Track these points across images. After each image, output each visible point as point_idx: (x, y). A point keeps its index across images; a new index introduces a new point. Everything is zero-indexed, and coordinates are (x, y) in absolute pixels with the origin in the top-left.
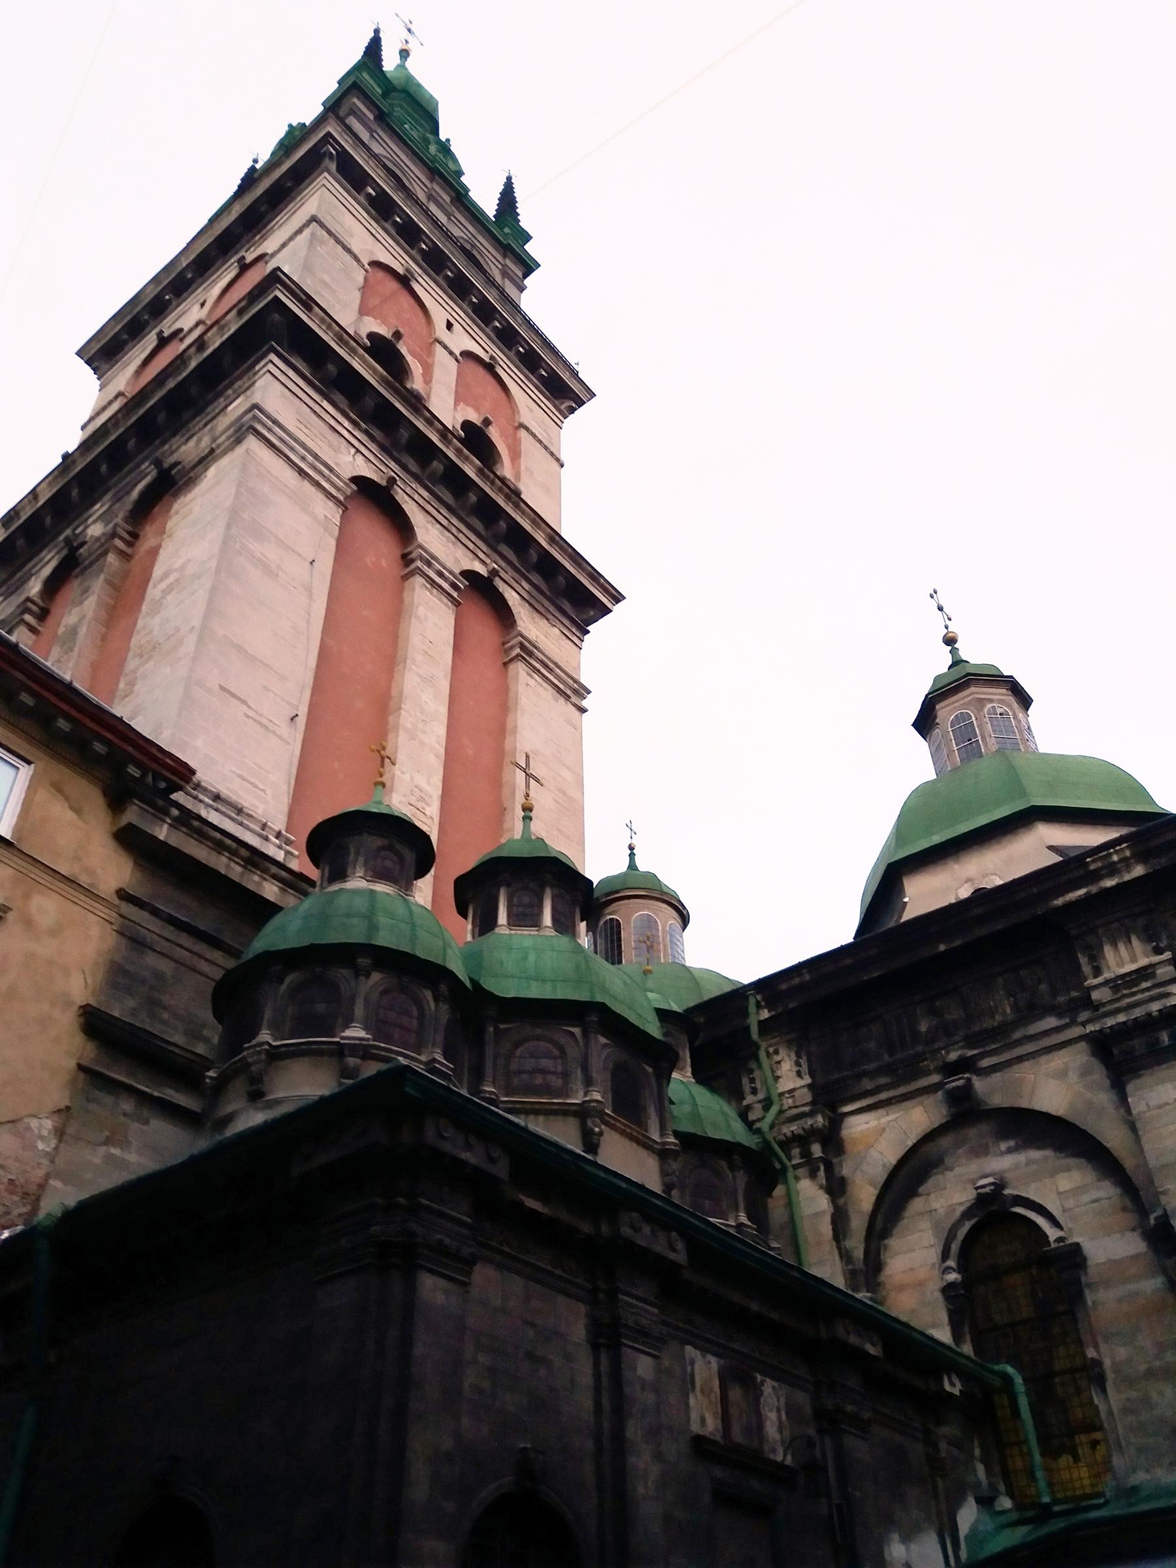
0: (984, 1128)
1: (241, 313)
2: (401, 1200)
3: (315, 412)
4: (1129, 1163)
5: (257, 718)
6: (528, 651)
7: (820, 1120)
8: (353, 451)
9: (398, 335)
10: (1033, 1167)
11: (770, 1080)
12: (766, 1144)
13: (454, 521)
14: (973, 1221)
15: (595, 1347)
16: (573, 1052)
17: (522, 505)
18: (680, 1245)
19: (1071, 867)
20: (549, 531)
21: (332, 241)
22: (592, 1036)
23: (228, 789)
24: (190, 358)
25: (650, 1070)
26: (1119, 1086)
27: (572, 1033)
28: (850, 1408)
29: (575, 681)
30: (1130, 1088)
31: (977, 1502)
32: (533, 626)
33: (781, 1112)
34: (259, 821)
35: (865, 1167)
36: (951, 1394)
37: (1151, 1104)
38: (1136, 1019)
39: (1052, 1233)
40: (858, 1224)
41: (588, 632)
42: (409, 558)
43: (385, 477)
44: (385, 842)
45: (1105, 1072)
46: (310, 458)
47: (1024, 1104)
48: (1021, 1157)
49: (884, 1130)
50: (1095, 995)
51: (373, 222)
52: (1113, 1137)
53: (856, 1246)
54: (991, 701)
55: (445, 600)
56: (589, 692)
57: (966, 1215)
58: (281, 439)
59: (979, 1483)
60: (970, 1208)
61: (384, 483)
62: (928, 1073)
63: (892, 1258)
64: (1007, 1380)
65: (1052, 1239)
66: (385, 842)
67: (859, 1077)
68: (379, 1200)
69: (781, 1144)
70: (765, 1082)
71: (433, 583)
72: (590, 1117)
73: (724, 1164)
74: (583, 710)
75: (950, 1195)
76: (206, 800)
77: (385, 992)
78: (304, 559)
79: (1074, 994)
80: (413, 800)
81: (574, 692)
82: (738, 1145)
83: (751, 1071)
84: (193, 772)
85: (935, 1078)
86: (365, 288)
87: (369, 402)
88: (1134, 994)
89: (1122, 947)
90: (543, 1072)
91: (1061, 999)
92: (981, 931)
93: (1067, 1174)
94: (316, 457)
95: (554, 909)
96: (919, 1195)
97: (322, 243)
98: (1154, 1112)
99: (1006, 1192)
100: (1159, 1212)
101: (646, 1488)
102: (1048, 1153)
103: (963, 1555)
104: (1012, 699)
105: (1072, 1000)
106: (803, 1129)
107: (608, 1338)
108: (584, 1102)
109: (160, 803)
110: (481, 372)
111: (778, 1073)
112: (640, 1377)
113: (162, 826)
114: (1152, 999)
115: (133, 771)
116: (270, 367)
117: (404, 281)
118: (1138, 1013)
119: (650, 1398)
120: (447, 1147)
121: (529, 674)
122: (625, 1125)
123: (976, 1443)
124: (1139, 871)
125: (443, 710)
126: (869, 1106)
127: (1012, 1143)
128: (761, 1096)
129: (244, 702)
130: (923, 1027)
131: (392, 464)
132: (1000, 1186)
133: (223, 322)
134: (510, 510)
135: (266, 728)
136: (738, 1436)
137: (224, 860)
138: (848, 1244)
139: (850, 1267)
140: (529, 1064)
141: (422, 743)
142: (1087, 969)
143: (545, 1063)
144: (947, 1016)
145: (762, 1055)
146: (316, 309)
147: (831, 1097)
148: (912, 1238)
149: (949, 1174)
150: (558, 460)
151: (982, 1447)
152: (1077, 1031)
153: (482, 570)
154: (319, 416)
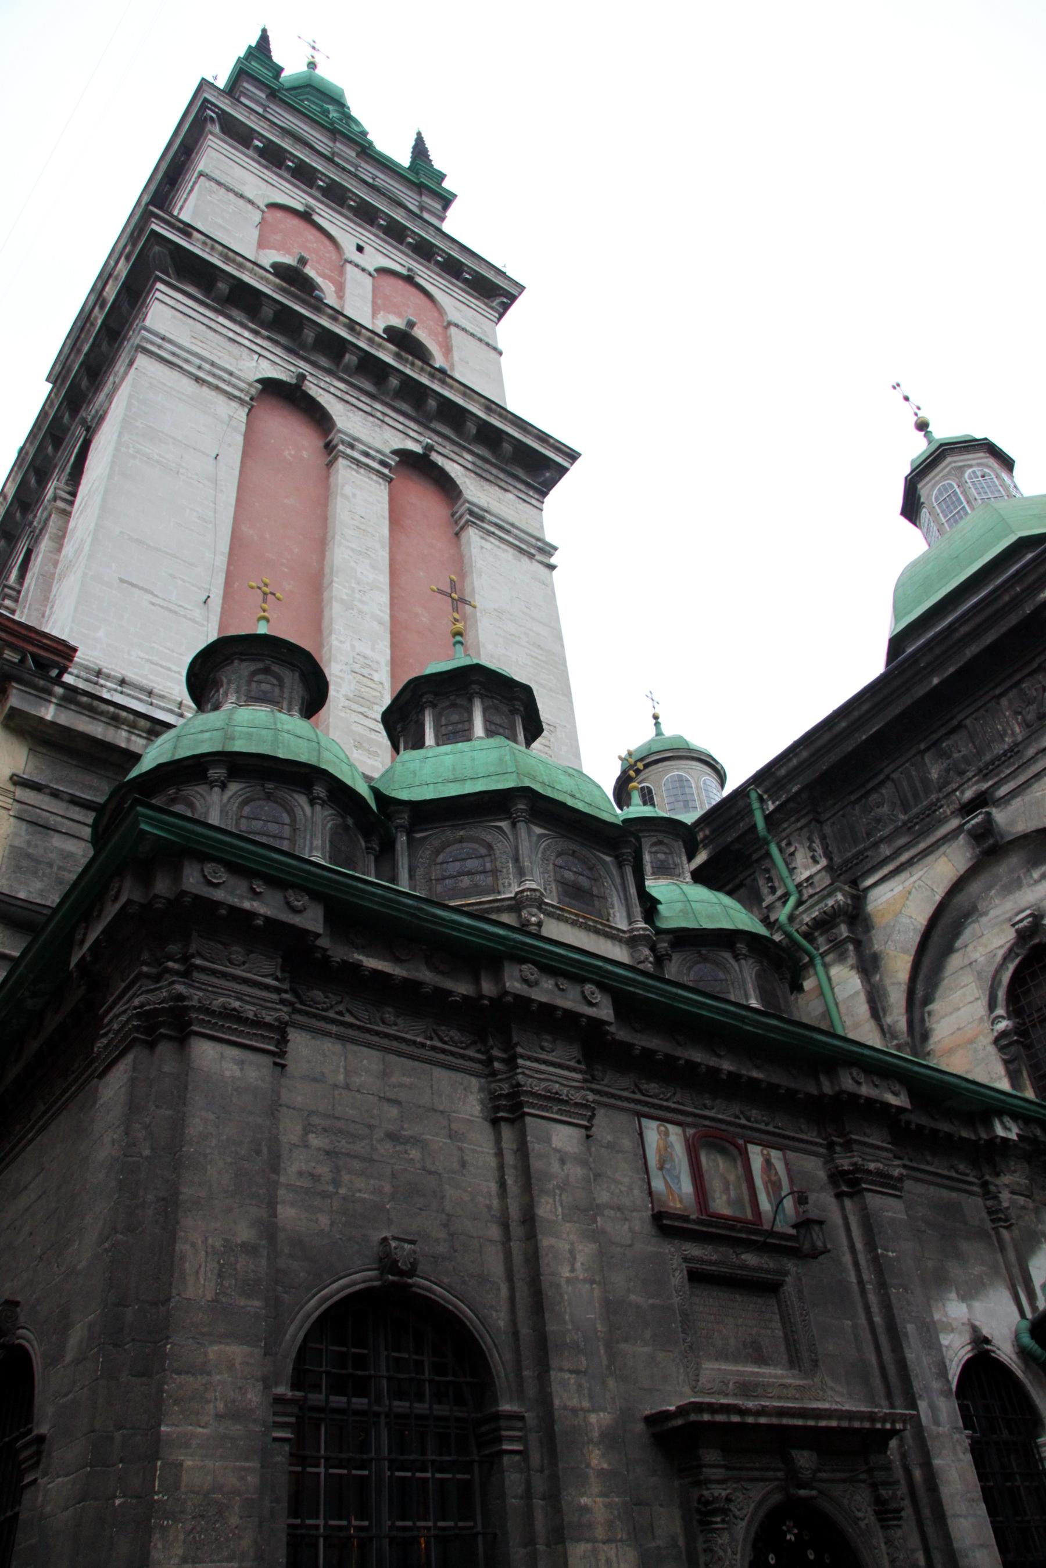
0: (1014, 860)
1: (128, 258)
2: (170, 964)
3: (210, 328)
5: (166, 604)
6: (478, 516)
8: (256, 357)
9: (303, 261)
13: (379, 406)
14: (1017, 961)
15: (495, 1122)
16: (501, 847)
17: (448, 380)
18: (598, 997)
20: (483, 400)
21: (223, 190)
22: (521, 825)
23: (136, 674)
24: (96, 318)
25: (608, 859)
27: (500, 828)
28: (872, 1166)
29: (538, 539)
32: (476, 491)
33: (800, 903)
34: (174, 701)
35: (896, 936)
36: (1005, 1140)
40: (897, 997)
42: (330, 445)
43: (294, 375)
44: (261, 666)
46: (207, 366)
49: (910, 893)
51: (265, 171)
53: (897, 1017)
55: (375, 477)
56: (556, 549)
58: (174, 354)
60: (1011, 950)
61: (294, 381)
62: (942, 821)
63: (938, 1022)
66: (261, 666)
67: (876, 845)
68: (145, 969)
69: (808, 936)
70: (782, 879)
71: (358, 463)
72: (525, 907)
73: (728, 955)
74: (552, 567)
76: (109, 684)
77: (246, 802)
78: (208, 456)
80: (356, 667)
81: (539, 551)
83: (767, 871)
84: (74, 650)
85: (955, 823)
86: (263, 223)
87: (268, 312)
90: (469, 873)
92: (971, 651)
94: (213, 364)
95: (486, 721)
96: (958, 950)
97: (211, 192)
101: (573, 1270)
106: (825, 912)
107: (508, 1110)
108: (517, 893)
109: (41, 683)
110: (400, 284)
112: (556, 1150)
113: (47, 709)
115: (8, 654)
116: (158, 295)
117: (306, 216)
119: (576, 1172)
120: (219, 895)
121: (482, 538)
122: (576, 915)
125: (384, 579)
126: (891, 872)
128: (779, 893)
129: (146, 591)
130: (934, 775)
131: (302, 364)
133: (116, 273)
134: (436, 387)
135: (176, 613)
137: (124, 734)
138: (889, 1020)
139: (895, 1042)
140: (454, 867)
141: (361, 612)
143: (471, 864)
144: (956, 755)
145: (774, 850)
146: (196, 234)
149: (984, 920)
150: (495, 349)
153: (418, 449)
154: (215, 331)
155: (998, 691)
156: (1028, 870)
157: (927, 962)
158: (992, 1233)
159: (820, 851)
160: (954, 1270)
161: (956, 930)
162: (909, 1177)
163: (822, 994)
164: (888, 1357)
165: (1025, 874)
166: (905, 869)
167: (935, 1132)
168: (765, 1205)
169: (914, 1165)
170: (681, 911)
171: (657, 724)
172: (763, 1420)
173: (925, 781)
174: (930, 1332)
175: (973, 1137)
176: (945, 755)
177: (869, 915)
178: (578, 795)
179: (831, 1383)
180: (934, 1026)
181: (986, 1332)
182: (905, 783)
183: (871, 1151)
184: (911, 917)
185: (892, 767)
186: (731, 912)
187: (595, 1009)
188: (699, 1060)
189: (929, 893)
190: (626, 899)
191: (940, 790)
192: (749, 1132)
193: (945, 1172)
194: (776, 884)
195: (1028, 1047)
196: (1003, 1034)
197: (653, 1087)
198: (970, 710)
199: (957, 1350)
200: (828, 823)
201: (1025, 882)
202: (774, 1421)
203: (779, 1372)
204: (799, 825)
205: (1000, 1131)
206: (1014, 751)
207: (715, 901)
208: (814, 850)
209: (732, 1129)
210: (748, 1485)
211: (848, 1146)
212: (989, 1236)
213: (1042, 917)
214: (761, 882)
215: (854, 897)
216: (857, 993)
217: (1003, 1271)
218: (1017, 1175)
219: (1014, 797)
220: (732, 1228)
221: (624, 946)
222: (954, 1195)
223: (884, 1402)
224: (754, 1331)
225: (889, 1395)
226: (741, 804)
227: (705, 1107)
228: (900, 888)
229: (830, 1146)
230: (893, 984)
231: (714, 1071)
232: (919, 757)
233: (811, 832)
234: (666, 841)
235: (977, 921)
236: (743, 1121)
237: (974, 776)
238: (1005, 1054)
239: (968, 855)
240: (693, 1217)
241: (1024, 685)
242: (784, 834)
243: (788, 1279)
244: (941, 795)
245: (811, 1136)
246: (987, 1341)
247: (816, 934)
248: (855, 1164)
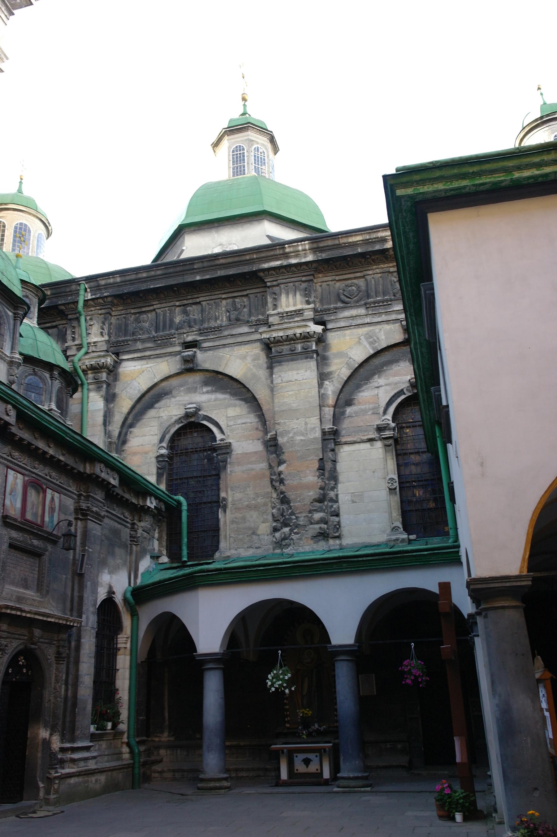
0: (196, 378)
4: (265, 408)
7: (109, 360)
10: (218, 402)
11: (84, 334)
12: (75, 369)
14: (181, 425)
18: (13, 413)
19: (276, 248)
25: (10, 314)
26: (270, 368)
28: (95, 509)
30: (275, 370)
31: (151, 557)
33: (87, 353)
35: (128, 390)
36: (149, 507)
37: (284, 380)
38: (287, 336)
39: (219, 436)
40: (118, 419)
41: (13, 14)
45: (266, 360)
47: (221, 370)
48: (213, 396)
50: (271, 319)
52: (261, 393)
54: (258, 143)
57: (177, 422)
59: (154, 549)
60: (180, 419)
62: (172, 345)
63: (133, 438)
64: (179, 503)
65: (218, 439)
67: (135, 340)
69: (83, 371)
70: (81, 336)
73: (48, 375)
75: (171, 411)
79: (261, 317)
82: (58, 366)
85: (178, 348)
88: (290, 323)
89: (291, 296)
91: (253, 318)
93: (233, 408)
98: (284, 384)
99: (200, 413)
100: (274, 433)
102: (227, 396)
103: (139, 581)
104: (269, 145)
105: (259, 320)
111: (89, 331)
114: (299, 327)
118: (290, 333)
123: (157, 531)
124: (310, 258)
127: (209, 388)
128: (77, 342)
130: (177, 320)
132: (198, 409)
136: (29, 516)
138: (110, 428)
139: (110, 440)
142: (270, 305)
145: (82, 319)
147: (117, 349)
148: (146, 430)
149: (173, 400)
151: (159, 533)
152: (257, 336)
155: (224, 296)
156: (202, 386)
157: (138, 407)
158: (129, 546)
159: (106, 331)
160: (111, 561)
161: (158, 398)
162: (108, 517)
163: (82, 403)
164: (76, 594)
165: (200, 387)
166: (146, 359)
167: (122, 497)
168: (47, 519)
169: (108, 510)
170: (31, 344)
171: (21, 183)
172: (28, 615)
173: (172, 321)
174: (95, 585)
175: (136, 503)
176: (185, 313)
177: (119, 373)
178: (5, 274)
179: (51, 602)
180: (131, 439)
181: (115, 590)
182: (161, 317)
183: (96, 502)
184: (139, 384)
185: (159, 306)
186: (56, 352)
187: (8, 418)
188: (41, 447)
189: (153, 376)
190: (13, 338)
191: (177, 330)
192: (49, 483)
193: (119, 515)
194: (77, 337)
195: (170, 465)
196: (162, 456)
197: (16, 454)
198: (207, 298)
199: (102, 595)
200: (115, 317)
201: (198, 390)
202: (32, 616)
203: (33, 594)
204: (100, 312)
205: (148, 504)
206: (219, 329)
207: (49, 344)
208: (103, 329)
209: (43, 480)
210: (13, 641)
211: (88, 497)
212: (127, 547)
213: (199, 410)
214: (69, 332)
215: (116, 362)
216: (99, 410)
217: (128, 564)
218: (147, 523)
219: (210, 350)
220: (33, 527)
221: (6, 364)
222: (120, 526)
223: (69, 613)
224: (27, 574)
225: (72, 610)
226: (74, 287)
227: (35, 468)
228: (140, 367)
229: (79, 496)
230: (119, 412)
231: (45, 453)
232: (173, 308)
233: (105, 319)
234: (30, 296)
235: (170, 399)
236: (48, 477)
237: (196, 331)
238: (159, 465)
239: (178, 367)
240: (19, 520)
241: (236, 300)
242: (90, 313)
243: (47, 553)
244: (177, 332)
245: (73, 489)
246: (114, 593)
247: (89, 372)
248: (88, 507)
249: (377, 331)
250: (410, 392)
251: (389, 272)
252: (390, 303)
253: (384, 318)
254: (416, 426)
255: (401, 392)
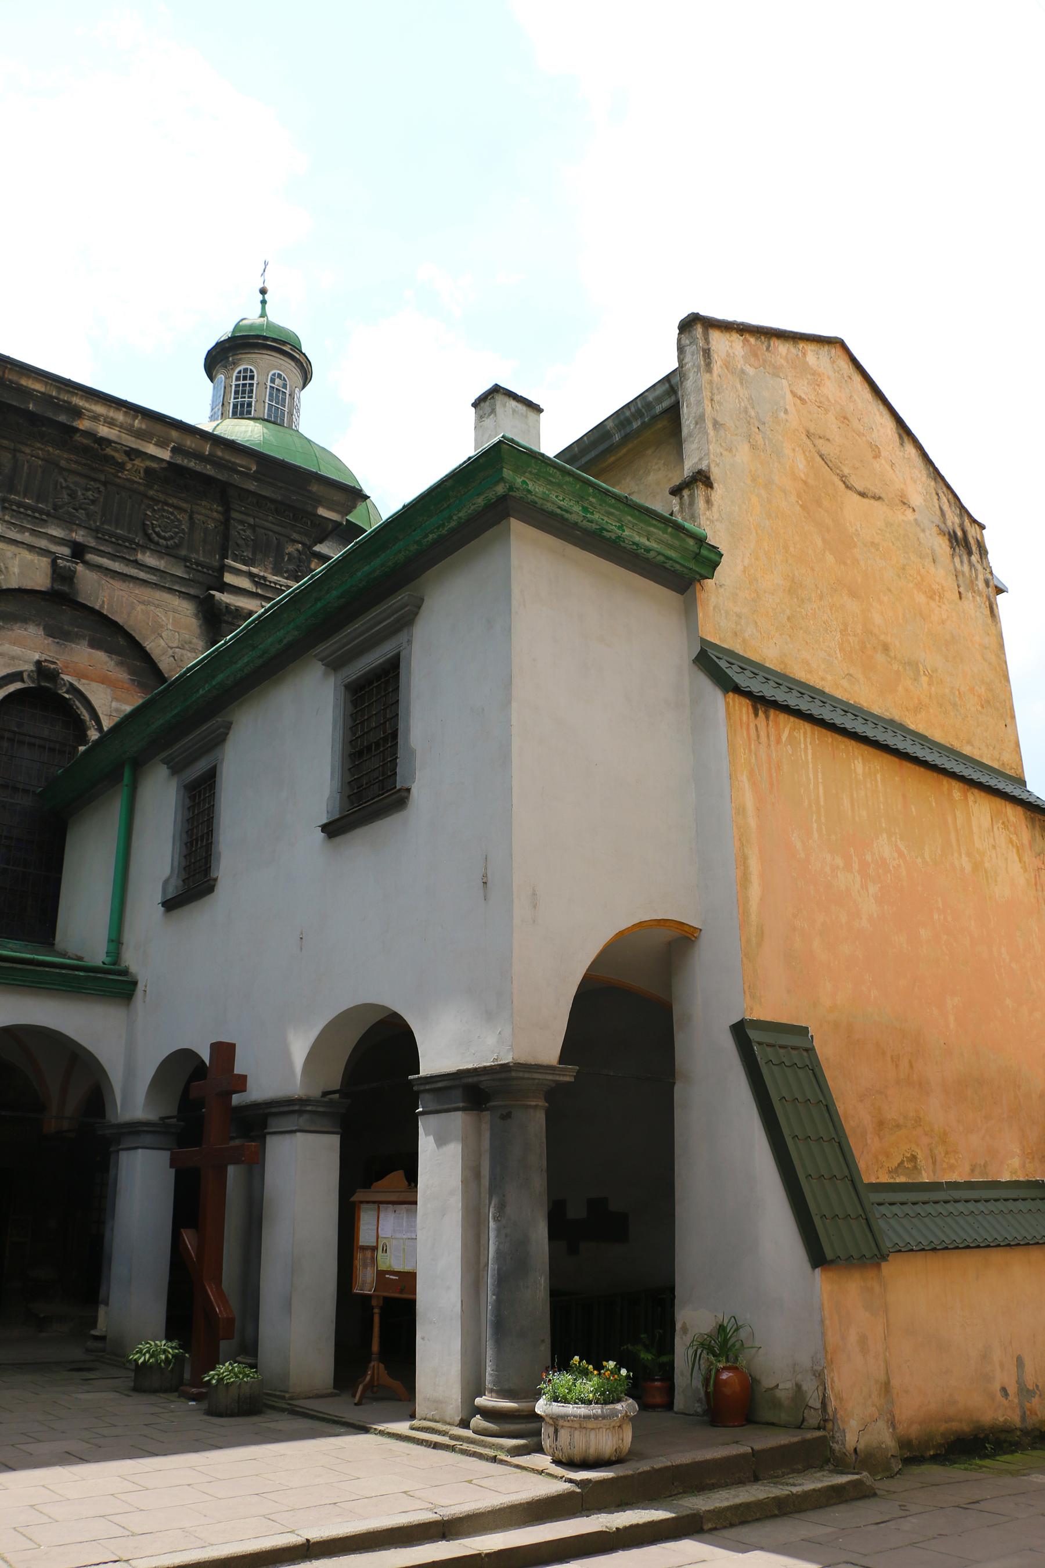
249: (9, 554)
250: (33, 682)
251: (57, 465)
252: (44, 517)
253: (26, 537)
254: (34, 745)
255: (17, 676)
